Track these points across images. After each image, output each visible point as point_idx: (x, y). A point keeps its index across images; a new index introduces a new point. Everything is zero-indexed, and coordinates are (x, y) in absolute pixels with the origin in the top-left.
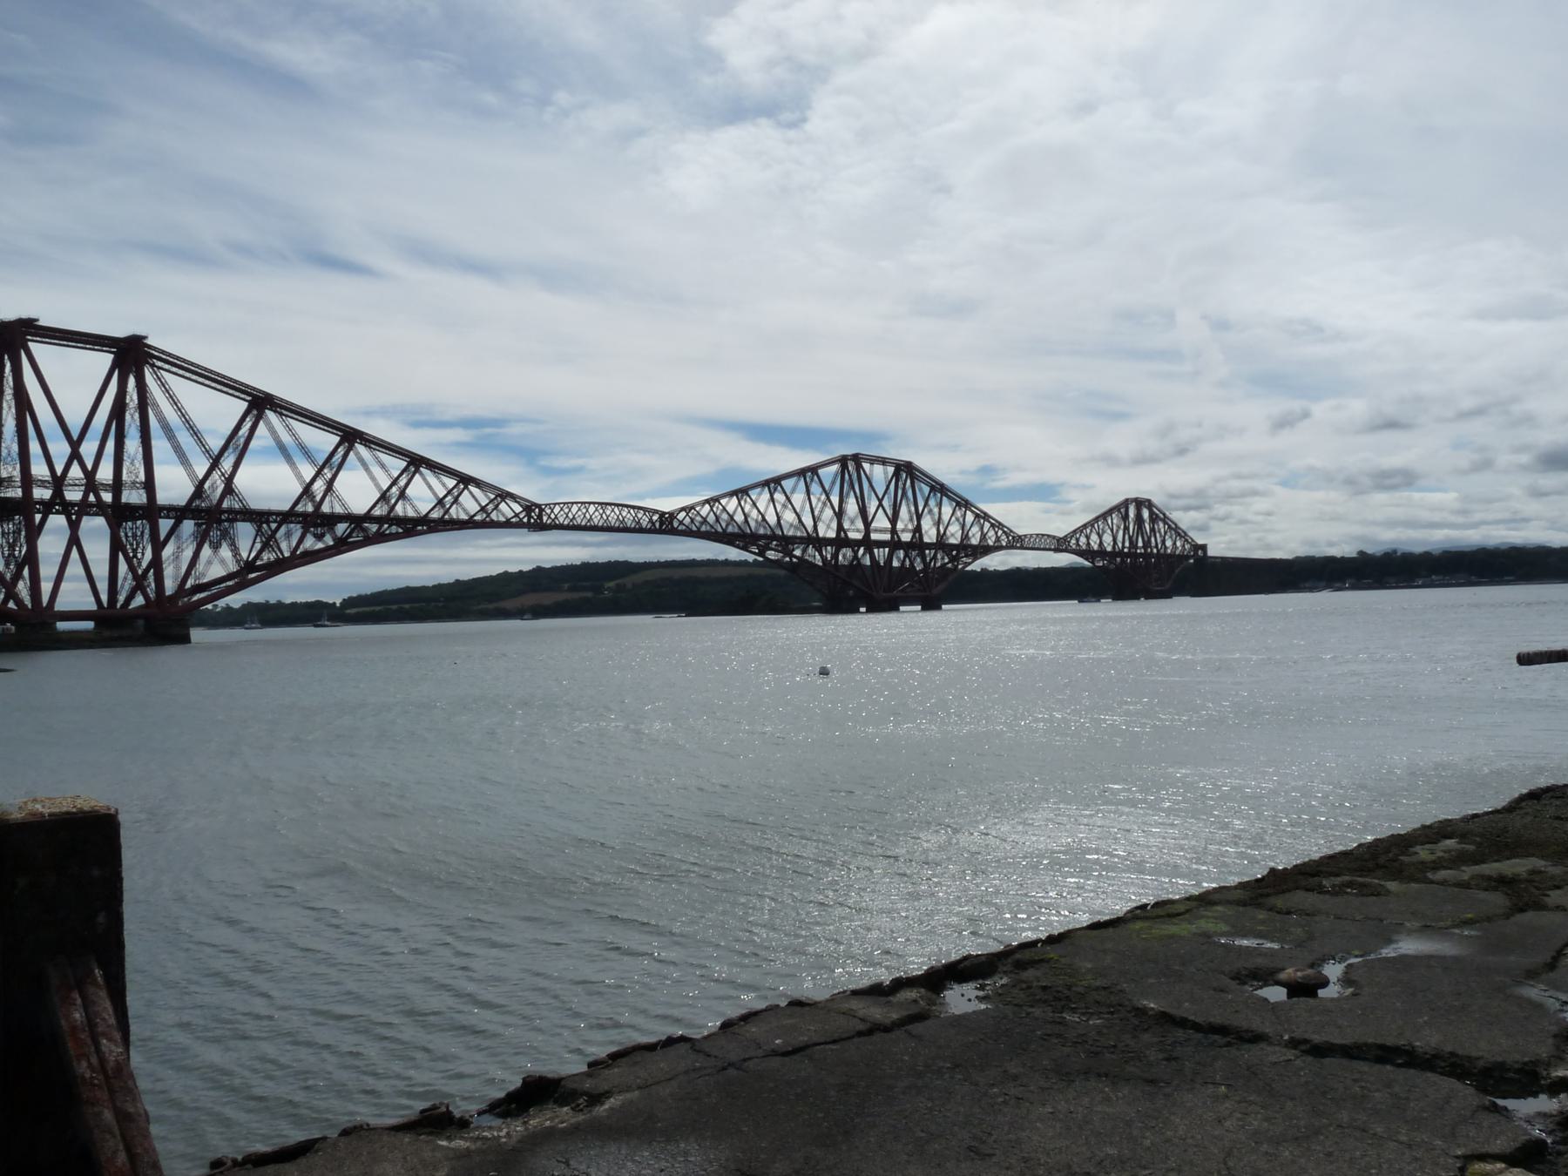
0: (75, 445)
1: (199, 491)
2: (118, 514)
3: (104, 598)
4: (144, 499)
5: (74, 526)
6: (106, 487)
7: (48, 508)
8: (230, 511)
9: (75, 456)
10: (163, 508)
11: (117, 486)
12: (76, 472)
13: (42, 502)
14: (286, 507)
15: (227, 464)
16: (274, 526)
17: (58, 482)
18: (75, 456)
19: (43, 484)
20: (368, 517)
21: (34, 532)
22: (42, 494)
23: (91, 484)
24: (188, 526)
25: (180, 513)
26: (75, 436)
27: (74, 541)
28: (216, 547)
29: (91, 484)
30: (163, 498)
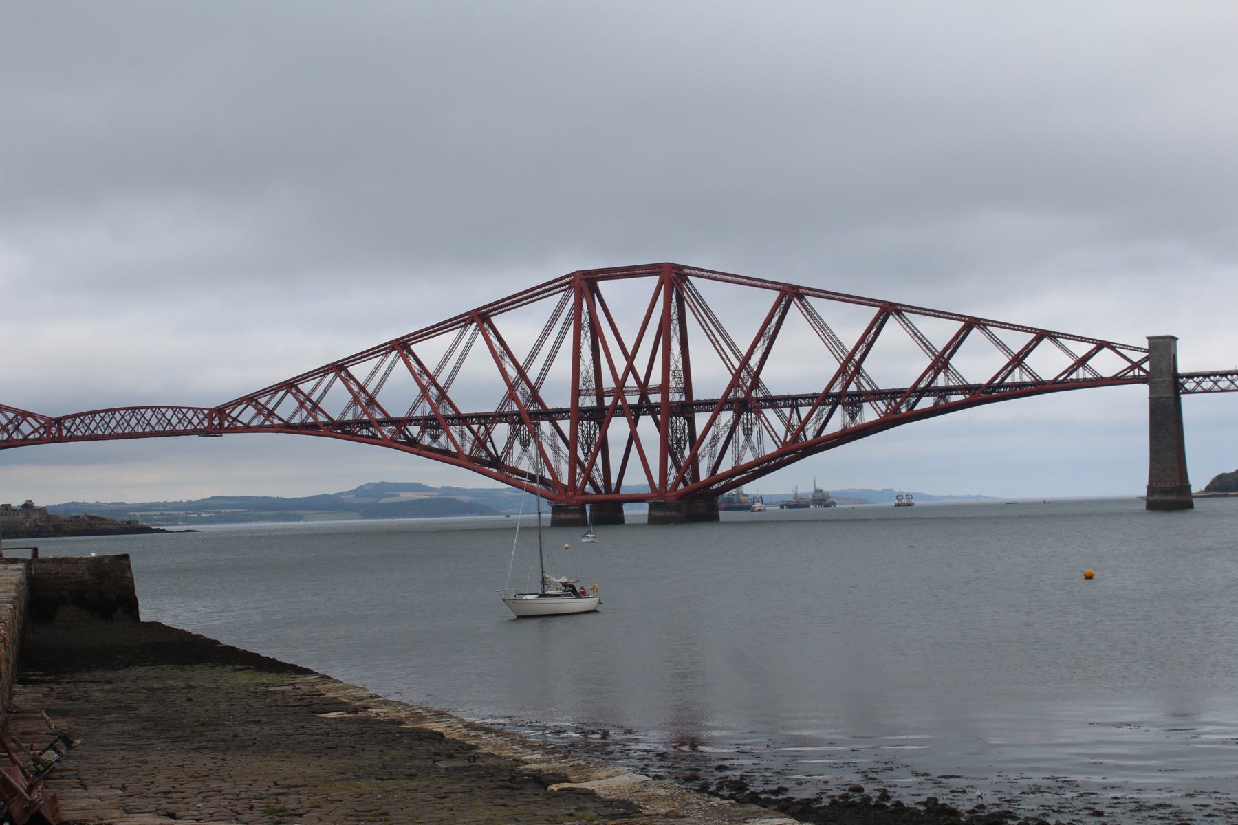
0: (630, 358)
1: (735, 383)
2: (664, 413)
3: (657, 481)
4: (683, 399)
5: (633, 424)
6: (654, 390)
7: (617, 411)
8: (758, 400)
9: (630, 368)
10: (699, 403)
11: (664, 388)
12: (631, 382)
13: (608, 408)
14: (820, 390)
15: (754, 361)
16: (804, 411)
17: (620, 390)
18: (630, 368)
19: (610, 393)
20: (917, 392)
23: (643, 389)
24: (726, 417)
25: (715, 407)
26: (630, 351)
27: (633, 437)
28: (748, 432)
29: (643, 389)
30: (697, 396)
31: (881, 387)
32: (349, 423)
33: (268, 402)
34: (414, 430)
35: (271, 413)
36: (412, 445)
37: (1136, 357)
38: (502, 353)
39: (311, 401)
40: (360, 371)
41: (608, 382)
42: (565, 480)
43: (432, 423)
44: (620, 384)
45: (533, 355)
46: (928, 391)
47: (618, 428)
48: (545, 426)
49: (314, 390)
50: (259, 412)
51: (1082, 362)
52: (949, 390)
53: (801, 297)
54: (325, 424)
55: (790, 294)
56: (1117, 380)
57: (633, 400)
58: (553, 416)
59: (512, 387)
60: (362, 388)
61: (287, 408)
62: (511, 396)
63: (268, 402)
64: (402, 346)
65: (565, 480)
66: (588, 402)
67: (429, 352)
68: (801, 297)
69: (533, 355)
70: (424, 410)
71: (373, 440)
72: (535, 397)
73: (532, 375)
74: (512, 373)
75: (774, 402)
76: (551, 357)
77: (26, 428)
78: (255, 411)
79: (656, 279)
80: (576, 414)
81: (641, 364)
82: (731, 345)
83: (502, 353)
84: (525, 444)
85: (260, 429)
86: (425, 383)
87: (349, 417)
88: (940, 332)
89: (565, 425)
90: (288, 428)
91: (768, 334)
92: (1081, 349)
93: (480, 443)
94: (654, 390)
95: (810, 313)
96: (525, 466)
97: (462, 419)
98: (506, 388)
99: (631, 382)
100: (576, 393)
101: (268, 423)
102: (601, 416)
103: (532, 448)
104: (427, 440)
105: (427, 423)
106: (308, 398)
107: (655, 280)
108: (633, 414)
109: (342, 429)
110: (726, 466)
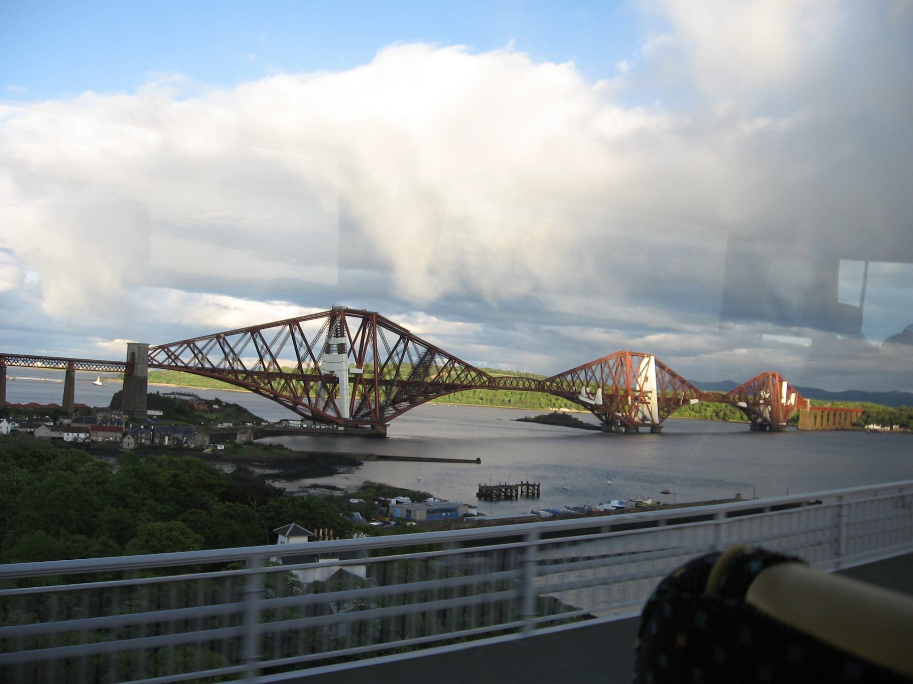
33: (176, 350)
35: (177, 358)
39: (202, 353)
40: (231, 340)
49: (204, 348)
50: (169, 357)
54: (208, 369)
60: (232, 350)
61: (187, 357)
63: (176, 350)
78: (167, 356)
85: (169, 367)
86: (263, 352)
87: (222, 366)
90: (186, 369)
98: (297, 362)
101: (173, 364)
106: (200, 352)
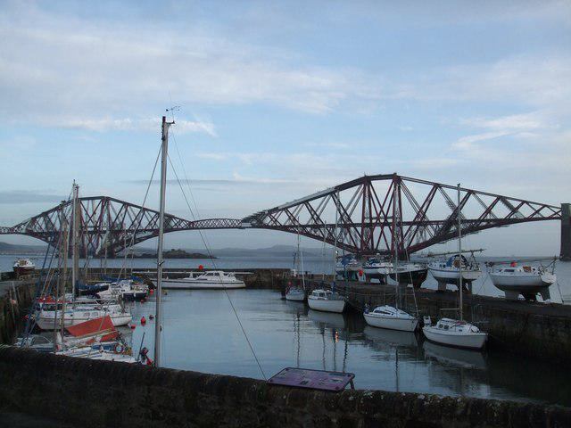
0: (382, 208)
1: (417, 216)
5: (382, 228)
6: (390, 218)
7: (376, 224)
9: (382, 211)
11: (393, 217)
12: (382, 215)
15: (424, 209)
17: (378, 218)
18: (382, 211)
20: (480, 220)
21: (372, 230)
22: (374, 221)
24: (414, 227)
27: (382, 232)
28: (421, 233)
29: (386, 217)
31: (468, 218)
32: (289, 226)
34: (309, 229)
36: (308, 234)
37: (557, 210)
38: (339, 204)
41: (374, 215)
42: (359, 247)
43: (316, 227)
44: (378, 215)
45: (349, 205)
46: (483, 221)
47: (377, 230)
48: (352, 229)
51: (537, 212)
52: (491, 220)
53: (440, 187)
55: (437, 186)
56: (550, 218)
57: (382, 221)
58: (355, 225)
59: (342, 216)
62: (342, 218)
64: (306, 202)
65: (359, 247)
66: (367, 221)
67: (314, 204)
68: (440, 187)
69: (349, 205)
70: (312, 222)
71: (295, 232)
72: (349, 219)
73: (348, 212)
74: (342, 211)
75: (430, 223)
76: (355, 206)
77: (182, 225)
79: (391, 181)
80: (363, 225)
81: (385, 209)
82: (416, 203)
83: (339, 204)
84: (345, 235)
88: (489, 201)
89: (359, 229)
91: (429, 200)
92: (537, 207)
93: (330, 234)
94: (390, 218)
95: (445, 195)
96: (346, 242)
97: (323, 225)
99: (382, 215)
100: (363, 218)
102: (371, 226)
103: (348, 236)
104: (313, 232)
105: (312, 227)
107: (391, 181)
108: (383, 225)
109: (284, 228)
110: (413, 243)
